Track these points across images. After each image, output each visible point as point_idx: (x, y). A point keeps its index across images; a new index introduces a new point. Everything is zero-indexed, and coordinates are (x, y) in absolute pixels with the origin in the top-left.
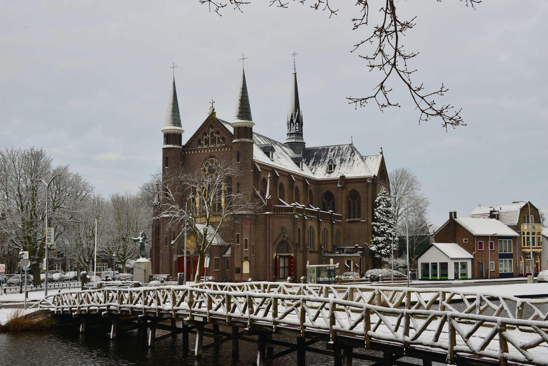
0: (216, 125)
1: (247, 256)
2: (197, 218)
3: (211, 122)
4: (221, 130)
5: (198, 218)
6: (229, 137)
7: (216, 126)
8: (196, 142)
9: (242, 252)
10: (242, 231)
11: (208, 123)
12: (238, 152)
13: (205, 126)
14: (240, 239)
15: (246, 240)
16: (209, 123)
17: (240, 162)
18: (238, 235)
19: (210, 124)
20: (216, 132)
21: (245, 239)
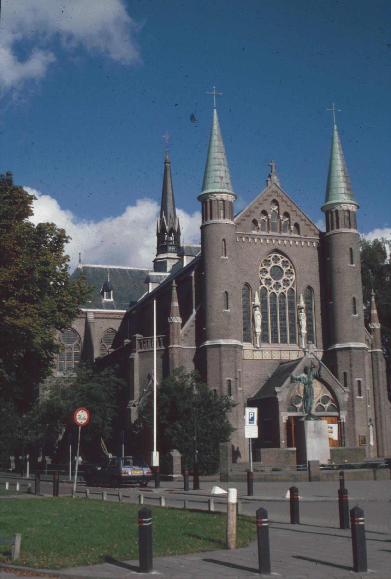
2: (256, 350)
3: (275, 197)
5: (257, 352)
8: (251, 224)
9: (367, 411)
10: (365, 375)
14: (363, 389)
18: (359, 382)
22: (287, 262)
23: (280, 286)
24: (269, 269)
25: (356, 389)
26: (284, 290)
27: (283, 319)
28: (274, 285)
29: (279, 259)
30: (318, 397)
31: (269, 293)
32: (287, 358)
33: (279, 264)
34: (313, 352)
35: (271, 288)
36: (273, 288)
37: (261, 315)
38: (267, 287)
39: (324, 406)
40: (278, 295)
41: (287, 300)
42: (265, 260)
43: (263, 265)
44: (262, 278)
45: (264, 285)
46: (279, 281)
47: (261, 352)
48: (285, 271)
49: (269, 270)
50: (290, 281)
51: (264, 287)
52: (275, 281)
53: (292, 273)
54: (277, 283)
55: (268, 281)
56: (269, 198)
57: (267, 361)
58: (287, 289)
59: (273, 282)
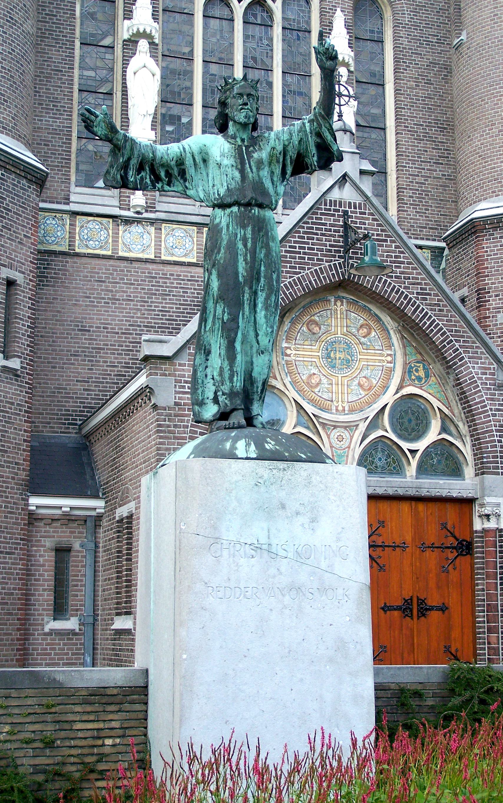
2: (128, 221)
5: (136, 229)
30: (377, 396)
34: (354, 175)
39: (405, 446)
41: (277, 31)
47: (152, 229)
57: (177, 268)
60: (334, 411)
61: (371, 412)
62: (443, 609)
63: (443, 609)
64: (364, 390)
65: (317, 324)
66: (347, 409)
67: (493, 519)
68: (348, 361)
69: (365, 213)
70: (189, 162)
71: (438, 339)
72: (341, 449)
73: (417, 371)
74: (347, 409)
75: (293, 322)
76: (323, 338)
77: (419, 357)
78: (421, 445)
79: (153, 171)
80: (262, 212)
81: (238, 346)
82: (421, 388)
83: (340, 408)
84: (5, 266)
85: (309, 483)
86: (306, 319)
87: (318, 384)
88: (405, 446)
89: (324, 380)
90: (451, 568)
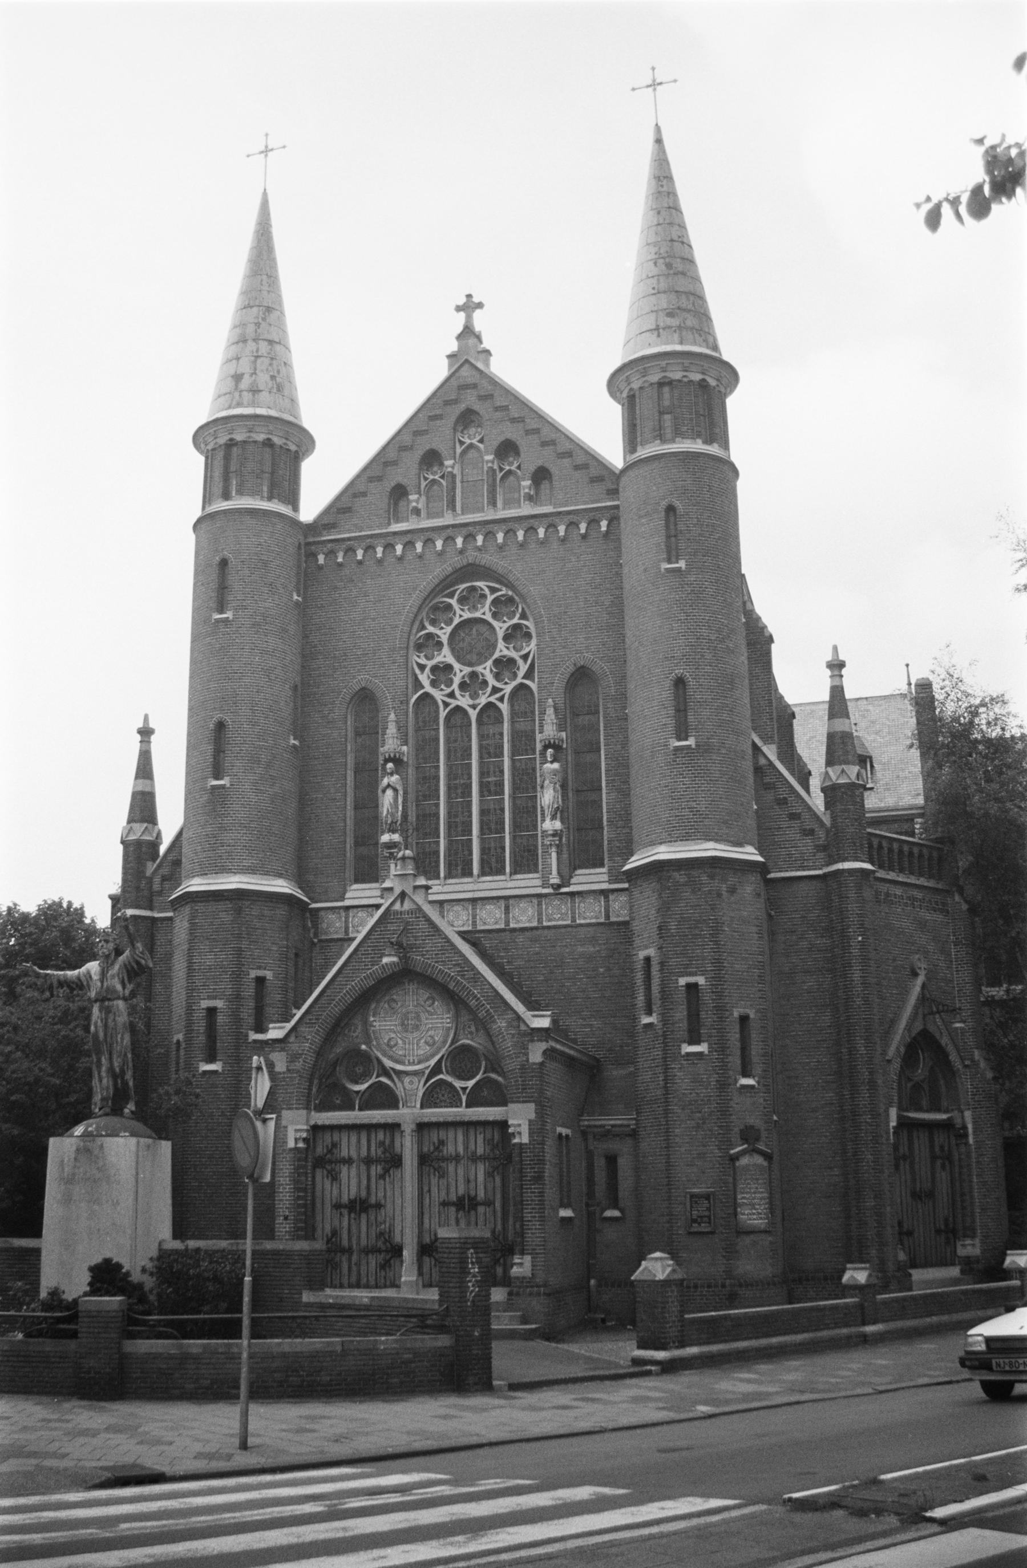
0: (497, 409)
1: (751, 1121)
3: (470, 400)
4: (528, 432)
6: (577, 468)
7: (499, 415)
11: (447, 403)
12: (670, 509)
13: (433, 418)
15: (744, 1019)
16: (456, 401)
17: (682, 564)
18: (692, 987)
19: (462, 407)
20: (495, 444)
21: (736, 1014)
22: (510, 600)
23: (485, 683)
24: (444, 634)
25: (680, 1014)
26: (498, 695)
27: (491, 788)
28: (463, 686)
29: (484, 596)
31: (443, 714)
32: (529, 921)
33: (485, 612)
34: (409, 891)
35: (452, 695)
36: (457, 693)
37: (400, 788)
38: (438, 695)
39: (458, 1084)
40: (473, 714)
42: (435, 608)
43: (427, 624)
44: (422, 667)
45: (428, 688)
46: (479, 669)
48: (500, 634)
49: (445, 639)
50: (520, 662)
51: (427, 695)
52: (467, 670)
53: (528, 636)
54: (473, 675)
55: (441, 672)
56: (449, 409)
58: (508, 689)
59: (460, 671)
60: (407, 1063)
61: (432, 1062)
62: (489, 1203)
63: (489, 1203)
64: (429, 1045)
65: (394, 1001)
66: (416, 1061)
67: (517, 1136)
68: (417, 1026)
69: (419, 917)
70: (83, 979)
71: (473, 1003)
72: (412, 1090)
73: (469, 1027)
74: (416, 1061)
75: (378, 1002)
76: (399, 1011)
77: (471, 1017)
78: (470, 1084)
79: (69, 986)
80: (111, 1003)
81: (104, 1074)
82: (472, 1040)
83: (411, 1061)
84: (253, 969)
85: (102, 1147)
86: (387, 998)
87: (396, 1045)
88: (458, 1084)
89: (400, 1042)
90: (496, 1173)
